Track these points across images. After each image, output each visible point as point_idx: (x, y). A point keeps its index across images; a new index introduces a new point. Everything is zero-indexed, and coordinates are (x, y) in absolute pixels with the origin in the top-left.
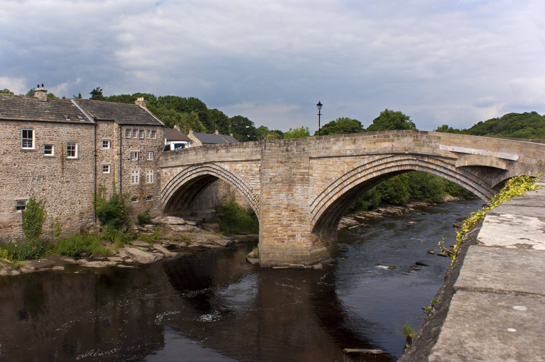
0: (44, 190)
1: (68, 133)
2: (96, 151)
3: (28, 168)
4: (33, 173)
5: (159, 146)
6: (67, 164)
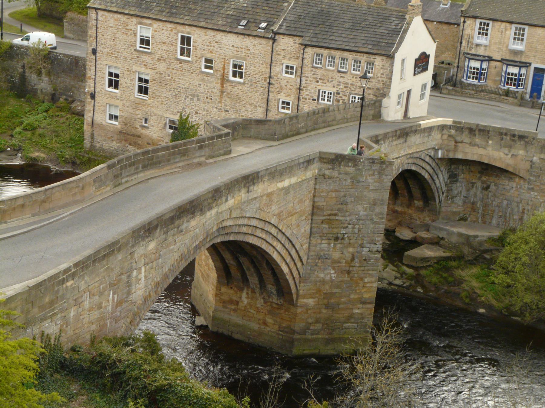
0: (197, 113)
1: (233, 46)
2: (270, 77)
3: (182, 82)
4: (186, 89)
5: (378, 89)
6: (227, 86)
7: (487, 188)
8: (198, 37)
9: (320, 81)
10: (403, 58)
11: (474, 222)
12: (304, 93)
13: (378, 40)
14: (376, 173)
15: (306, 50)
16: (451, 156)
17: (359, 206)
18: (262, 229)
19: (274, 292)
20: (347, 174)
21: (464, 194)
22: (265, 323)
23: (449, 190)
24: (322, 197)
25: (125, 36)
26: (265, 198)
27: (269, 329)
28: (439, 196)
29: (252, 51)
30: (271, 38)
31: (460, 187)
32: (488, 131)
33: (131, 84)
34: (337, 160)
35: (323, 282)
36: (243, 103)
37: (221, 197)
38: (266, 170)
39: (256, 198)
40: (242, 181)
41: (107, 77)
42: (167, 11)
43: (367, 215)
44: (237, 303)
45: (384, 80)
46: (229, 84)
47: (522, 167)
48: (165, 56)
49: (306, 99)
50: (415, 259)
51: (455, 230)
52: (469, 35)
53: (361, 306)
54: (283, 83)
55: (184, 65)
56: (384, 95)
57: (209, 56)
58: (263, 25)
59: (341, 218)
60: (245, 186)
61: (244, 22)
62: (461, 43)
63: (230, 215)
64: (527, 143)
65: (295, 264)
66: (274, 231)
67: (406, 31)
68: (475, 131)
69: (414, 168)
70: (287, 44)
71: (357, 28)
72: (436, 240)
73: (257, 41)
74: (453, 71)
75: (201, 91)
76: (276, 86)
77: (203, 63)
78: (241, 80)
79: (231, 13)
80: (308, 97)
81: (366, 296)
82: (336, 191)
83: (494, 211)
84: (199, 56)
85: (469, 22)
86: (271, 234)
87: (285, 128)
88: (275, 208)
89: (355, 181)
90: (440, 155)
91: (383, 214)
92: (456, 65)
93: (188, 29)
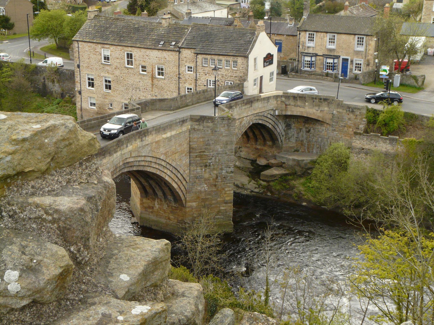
1: (156, 57)
2: (179, 74)
3: (129, 81)
5: (241, 77)
6: (155, 81)
7: (309, 131)
8: (136, 53)
9: (208, 74)
10: (255, 57)
11: (303, 152)
12: (199, 82)
13: (239, 48)
14: (226, 125)
15: (198, 56)
16: (284, 113)
17: (217, 146)
18: (155, 163)
19: (172, 200)
20: (208, 127)
21: (296, 135)
22: (169, 219)
23: (287, 134)
24: (195, 141)
25: (95, 56)
26: (154, 144)
27: (171, 222)
28: (281, 138)
29: (168, 59)
30: (178, 51)
31: (293, 132)
32: (305, 98)
33: (100, 83)
34: (202, 119)
35: (200, 192)
36: (165, 90)
37: (123, 145)
38: (153, 127)
39: (148, 145)
40: (137, 135)
41: (87, 81)
42: (118, 39)
43: (223, 151)
44: (153, 208)
45: (244, 71)
46: (156, 80)
47: (327, 117)
48: (119, 66)
49: (200, 85)
50: (267, 176)
51: (291, 157)
52: (303, 42)
53: (225, 205)
54: (187, 77)
55: (130, 70)
56: (245, 80)
57: (143, 64)
58: (173, 43)
59: (207, 154)
60: (139, 138)
61: (162, 43)
62: (299, 47)
63: (131, 155)
64: (329, 103)
65: (181, 182)
66: (163, 163)
67: (255, 41)
68: (297, 98)
69: (260, 122)
70: (187, 53)
71: (227, 41)
72: (280, 164)
73: (170, 53)
74: (295, 64)
75: (141, 85)
76: (183, 79)
77: (141, 69)
78: (163, 77)
79: (155, 37)
80: (201, 84)
81: (227, 199)
82: (203, 138)
83: (314, 145)
84: (138, 65)
85: (302, 34)
86: (162, 165)
87: (178, 103)
88: (162, 150)
89: (214, 131)
90: (277, 113)
91: (232, 150)
92: (297, 60)
93: (130, 49)
